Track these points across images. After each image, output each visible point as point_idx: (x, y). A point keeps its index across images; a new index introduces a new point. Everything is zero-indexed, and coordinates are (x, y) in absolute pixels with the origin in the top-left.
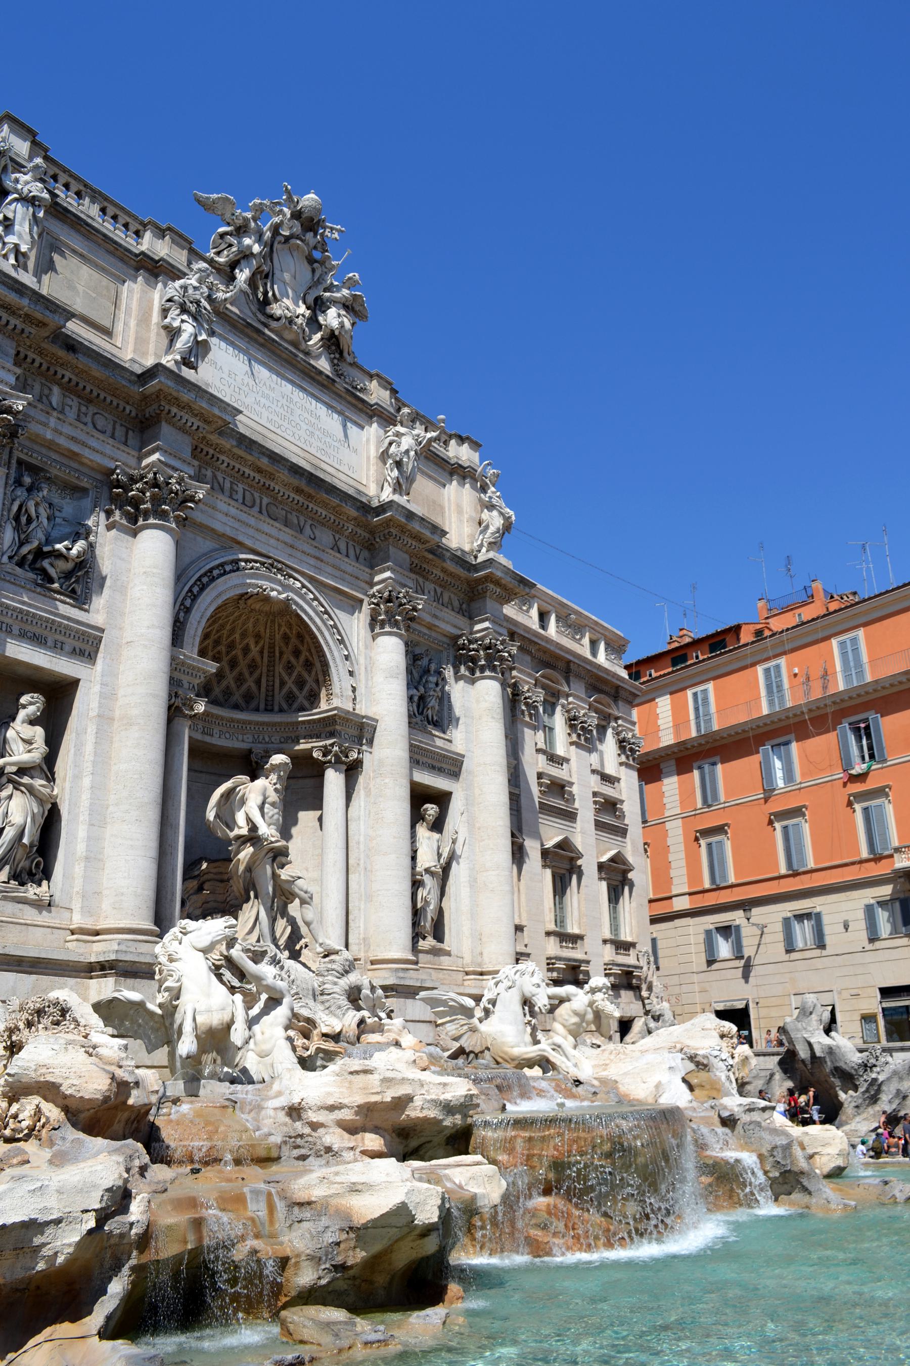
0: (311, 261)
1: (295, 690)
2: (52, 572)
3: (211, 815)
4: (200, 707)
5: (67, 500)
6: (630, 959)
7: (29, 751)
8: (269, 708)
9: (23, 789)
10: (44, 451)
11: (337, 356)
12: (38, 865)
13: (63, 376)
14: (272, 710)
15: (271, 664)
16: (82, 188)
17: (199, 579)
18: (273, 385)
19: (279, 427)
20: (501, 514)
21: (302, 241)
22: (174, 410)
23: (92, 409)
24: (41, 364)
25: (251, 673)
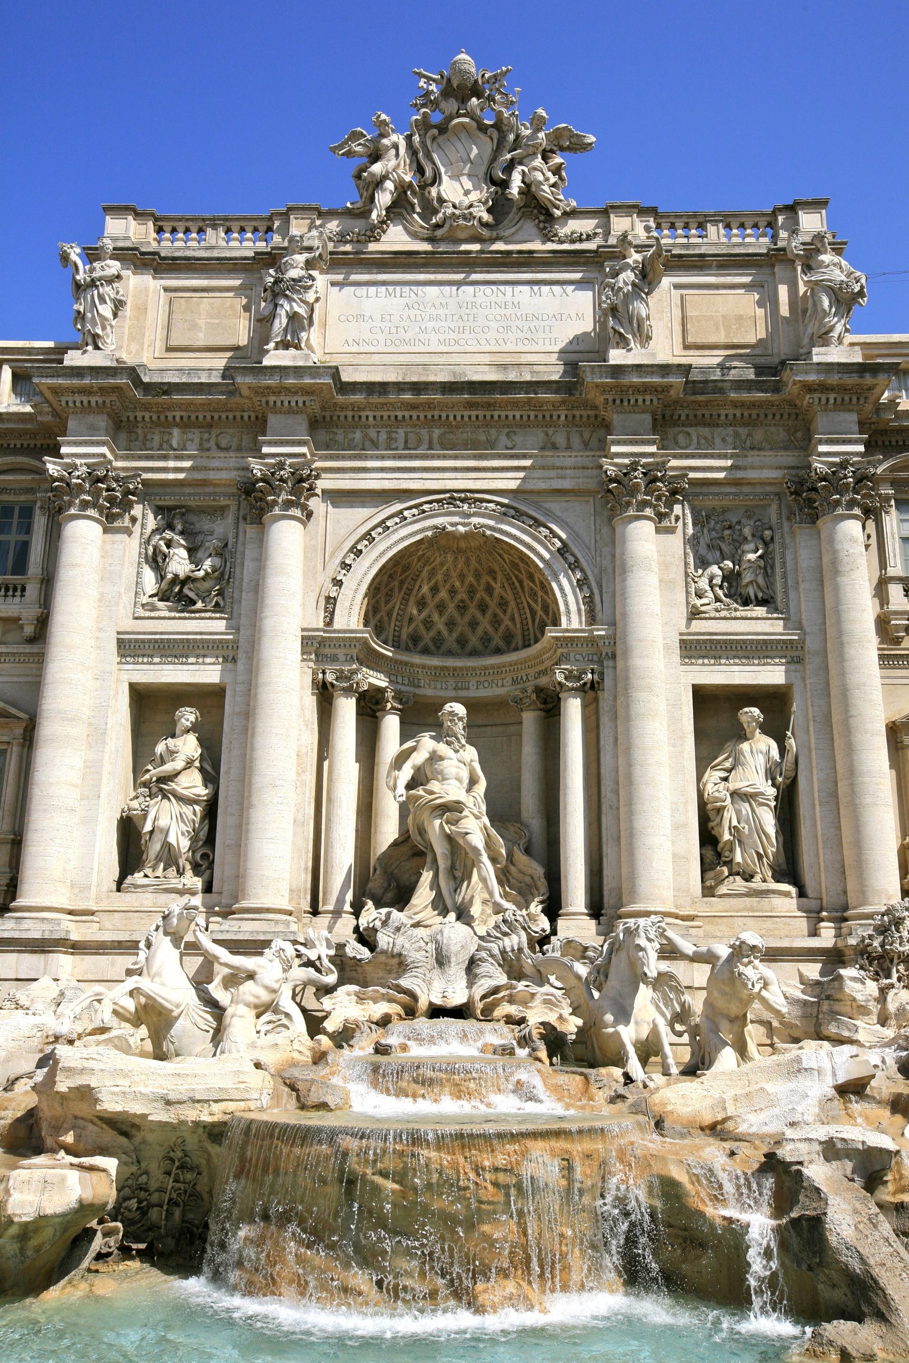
1: (544, 617)
2: (192, 595)
5: (219, 522)
10: (177, 490)
11: (542, 218)
12: (204, 856)
13: (174, 417)
14: (529, 645)
15: (516, 597)
16: (201, 224)
17: (354, 547)
18: (444, 302)
19: (457, 342)
21: (464, 115)
22: (272, 399)
23: (214, 432)
24: (151, 417)
25: (505, 612)
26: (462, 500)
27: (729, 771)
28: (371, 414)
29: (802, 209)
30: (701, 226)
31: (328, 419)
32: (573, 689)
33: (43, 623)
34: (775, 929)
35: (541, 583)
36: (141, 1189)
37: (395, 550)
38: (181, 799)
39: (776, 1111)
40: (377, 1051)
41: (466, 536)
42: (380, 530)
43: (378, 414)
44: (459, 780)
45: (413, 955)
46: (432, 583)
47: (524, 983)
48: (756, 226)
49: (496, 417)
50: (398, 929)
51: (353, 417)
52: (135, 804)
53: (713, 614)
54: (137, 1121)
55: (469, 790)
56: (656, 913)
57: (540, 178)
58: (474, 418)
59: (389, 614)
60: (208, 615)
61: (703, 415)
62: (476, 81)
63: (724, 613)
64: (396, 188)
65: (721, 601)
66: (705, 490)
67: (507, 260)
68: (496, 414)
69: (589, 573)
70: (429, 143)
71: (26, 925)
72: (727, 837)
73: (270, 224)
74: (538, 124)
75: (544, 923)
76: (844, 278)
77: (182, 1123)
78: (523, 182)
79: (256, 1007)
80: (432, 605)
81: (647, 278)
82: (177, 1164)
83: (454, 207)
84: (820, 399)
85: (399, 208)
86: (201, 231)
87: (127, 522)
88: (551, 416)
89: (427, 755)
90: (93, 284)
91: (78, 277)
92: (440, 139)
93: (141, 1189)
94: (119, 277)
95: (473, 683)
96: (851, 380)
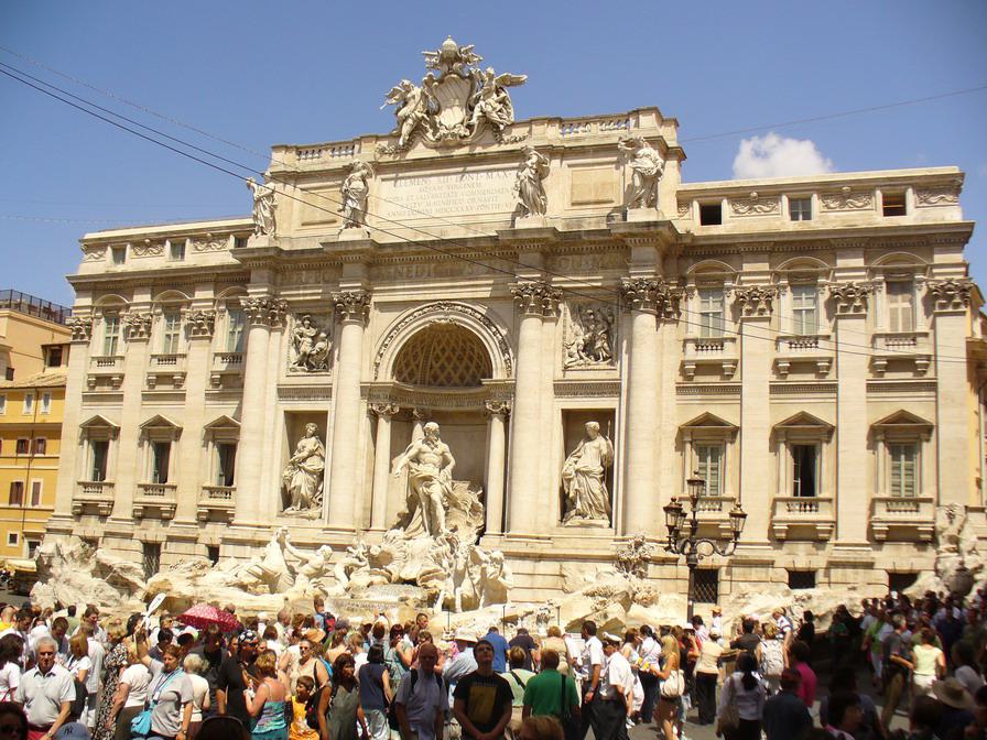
0: (463, 78)
6: (925, 513)
26: (445, 305)
27: (579, 457)
37: (408, 337)
38: (306, 471)
41: (448, 324)
45: (396, 554)
52: (286, 473)
57: (489, 109)
59: (417, 366)
64: (414, 121)
72: (571, 495)
74: (491, 77)
79: (308, 575)
80: (443, 360)
81: (541, 173)
85: (418, 130)
87: (280, 326)
90: (259, 200)
92: (441, 86)
96: (645, 230)
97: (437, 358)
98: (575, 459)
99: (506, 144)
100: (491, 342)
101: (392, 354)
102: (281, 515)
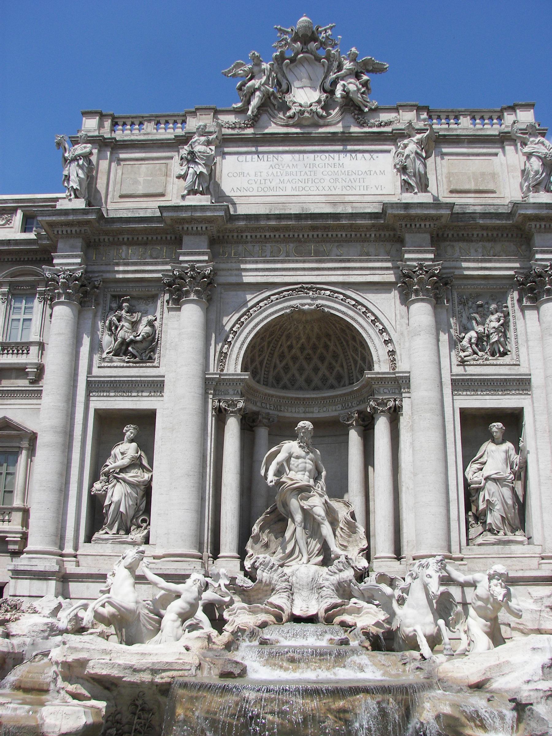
0: (318, 59)
1: (363, 364)
3: (263, 472)
4: (241, 405)
7: (122, 459)
8: (351, 382)
9: (120, 480)
10: (125, 285)
11: (356, 112)
13: (123, 239)
14: (353, 383)
20: (539, 157)
21: (306, 52)
22: (186, 226)
24: (109, 239)
25: (337, 361)
26: (309, 289)
27: (485, 463)
28: (249, 235)
29: (519, 109)
30: (457, 118)
31: (221, 238)
32: (382, 411)
33: (40, 369)
34: (513, 565)
35: (361, 342)
36: (118, 723)
37: (265, 322)
39: (515, 674)
40: (261, 643)
41: (311, 312)
42: (255, 309)
43: (254, 235)
44: (310, 472)
46: (289, 343)
47: (353, 600)
48: (491, 118)
49: (330, 236)
50: (272, 568)
51: (237, 236)
53: (472, 363)
54: (115, 681)
55: (316, 479)
56: (439, 555)
58: (315, 236)
59: (261, 363)
60: (144, 365)
61: (463, 235)
62: (313, 32)
63: (480, 362)
64: (264, 95)
65: (477, 354)
66: (465, 282)
67: (335, 138)
68: (330, 234)
69: (392, 336)
70: (284, 68)
71: (34, 562)
72: (482, 506)
73: (184, 118)
75: (364, 563)
76: (546, 151)
77: (143, 682)
78: (344, 91)
82: (139, 708)
83: (301, 105)
84: (536, 225)
86: (141, 124)
88: (366, 235)
89: (287, 455)
91: (67, 155)
93: (118, 723)
94: (91, 153)
95: (316, 409)
97: (282, 356)
98: (478, 466)
99: (371, 127)
100: (371, 331)
101: (243, 342)
102: (88, 539)
